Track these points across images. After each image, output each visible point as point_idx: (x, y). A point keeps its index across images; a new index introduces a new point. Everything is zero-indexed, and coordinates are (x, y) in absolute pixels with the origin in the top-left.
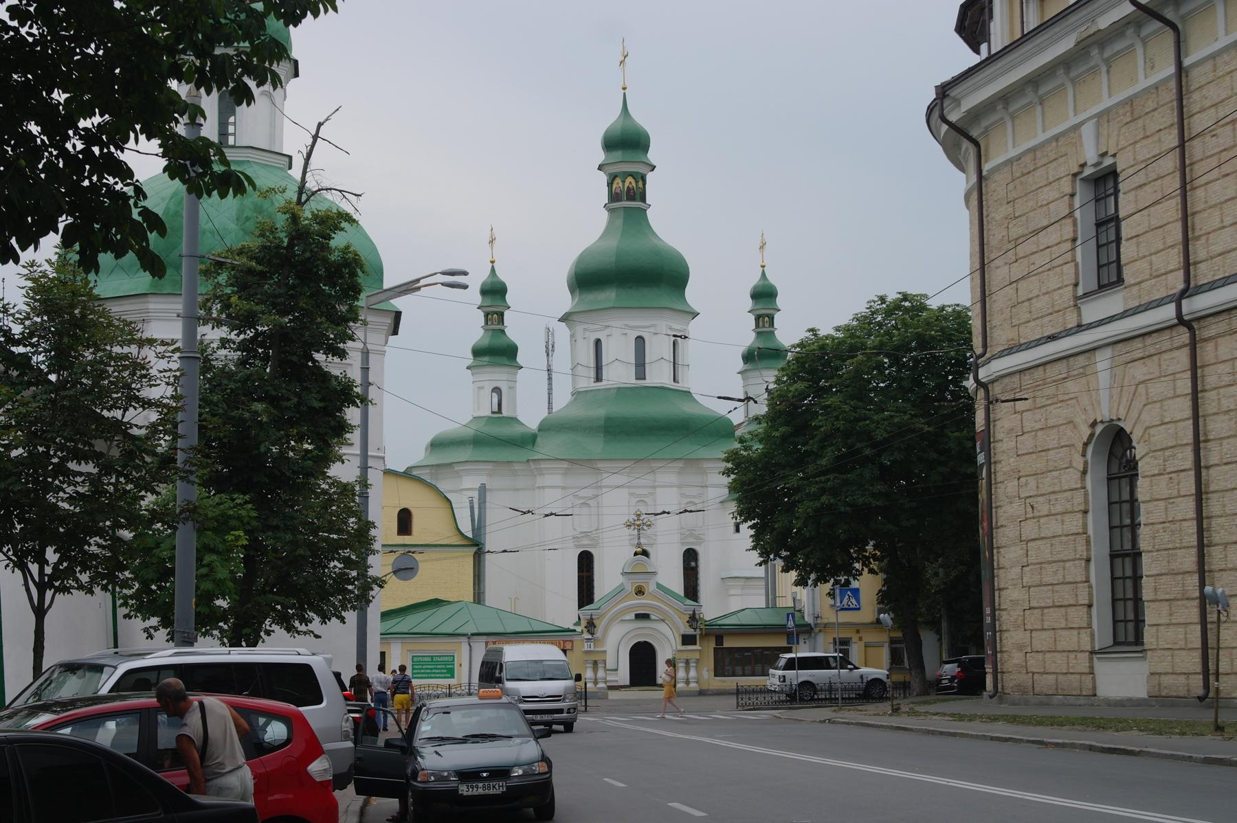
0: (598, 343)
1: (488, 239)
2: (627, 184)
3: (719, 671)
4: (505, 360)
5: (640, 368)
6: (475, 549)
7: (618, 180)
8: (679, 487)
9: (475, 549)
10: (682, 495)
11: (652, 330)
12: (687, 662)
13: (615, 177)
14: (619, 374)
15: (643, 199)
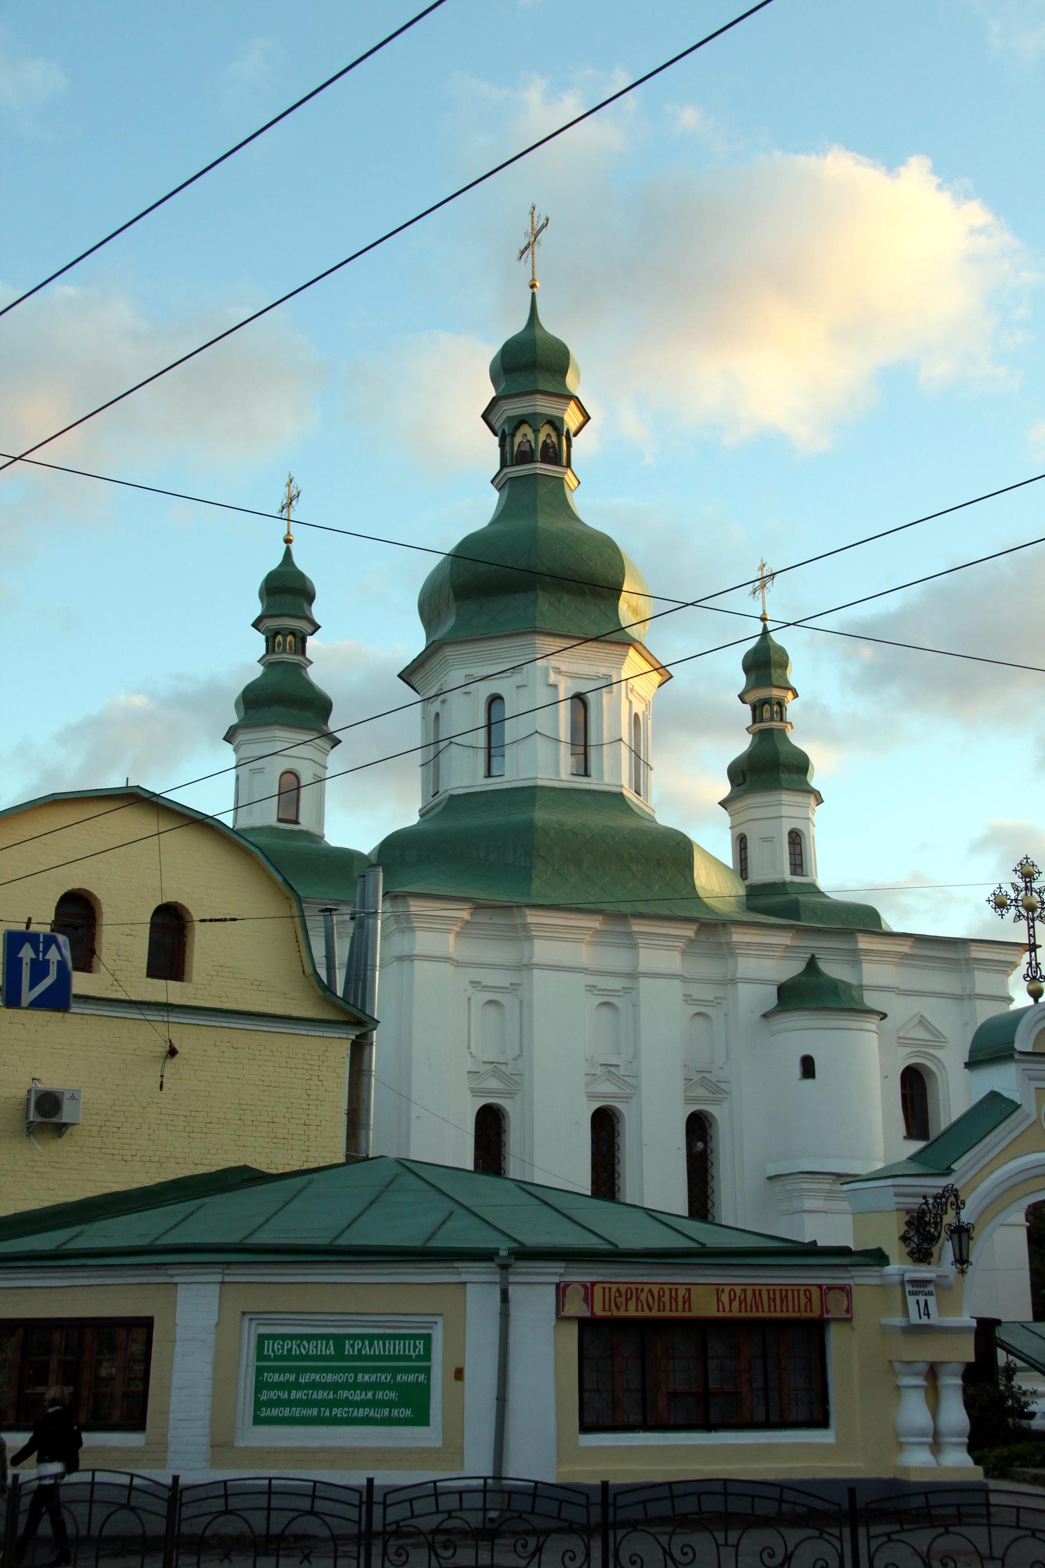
2: (542, 437)
7: (525, 429)
8: (684, 979)
10: (688, 998)
13: (517, 428)
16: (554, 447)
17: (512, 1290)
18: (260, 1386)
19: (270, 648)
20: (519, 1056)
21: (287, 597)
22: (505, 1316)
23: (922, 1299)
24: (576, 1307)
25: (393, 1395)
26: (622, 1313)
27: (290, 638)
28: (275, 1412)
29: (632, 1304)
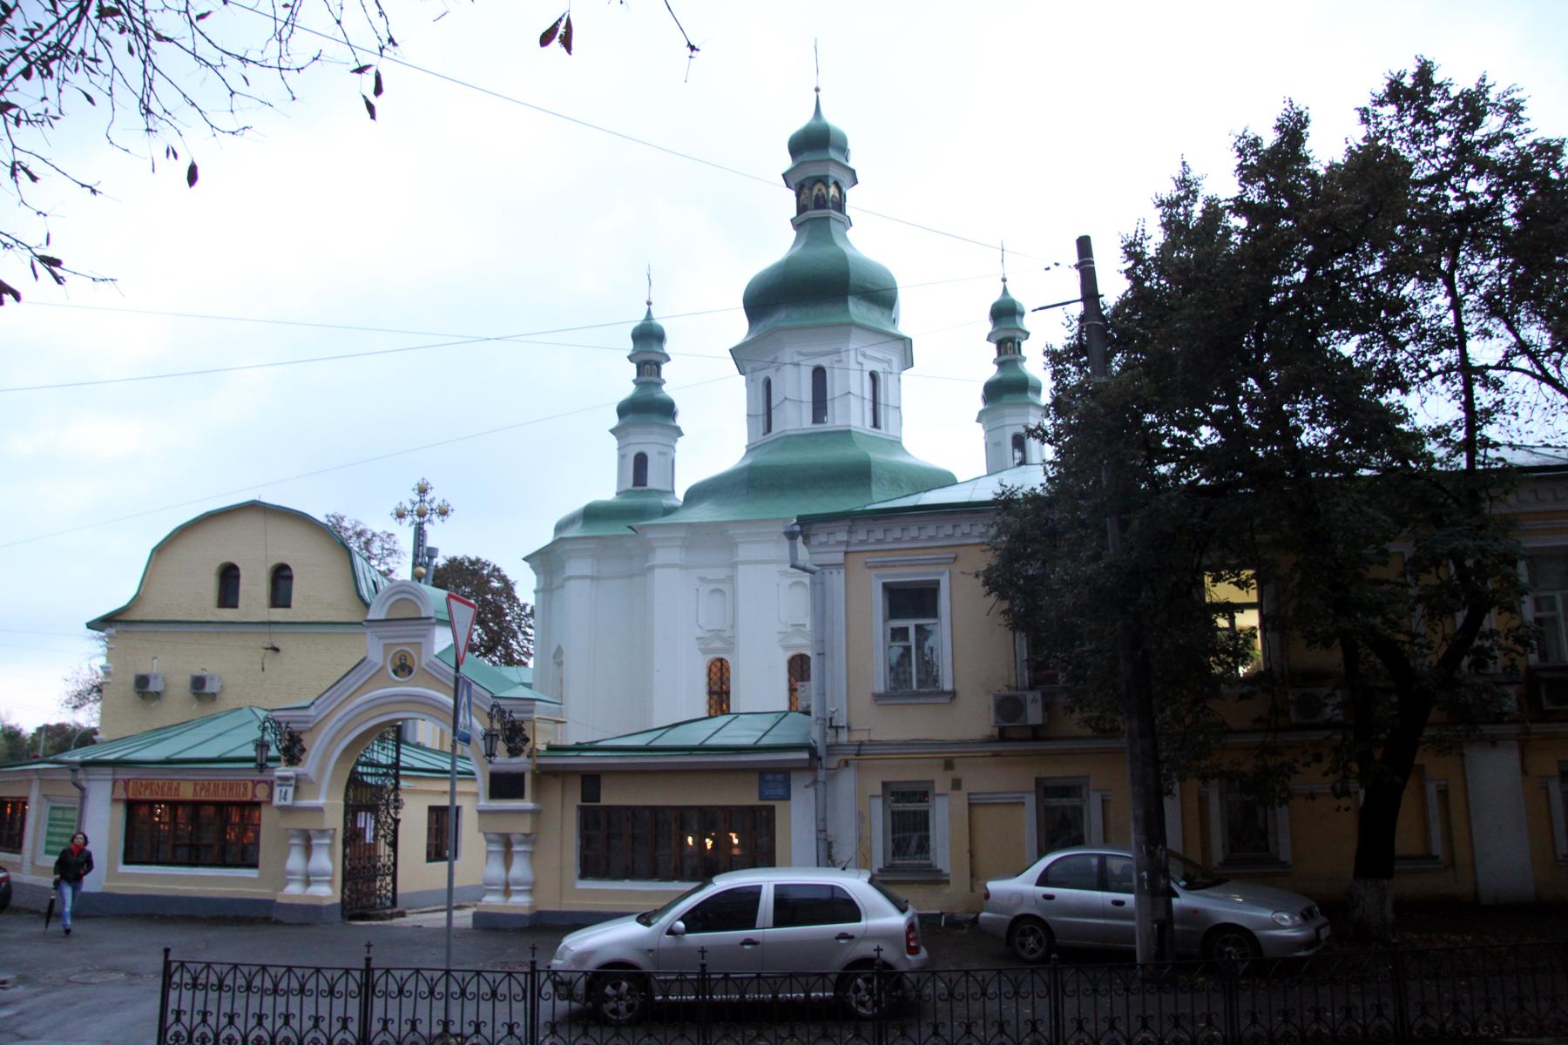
4: (656, 418)
5: (820, 407)
11: (835, 357)
12: (507, 842)
14: (795, 417)
17: (84, 784)
20: (733, 626)
21: (648, 339)
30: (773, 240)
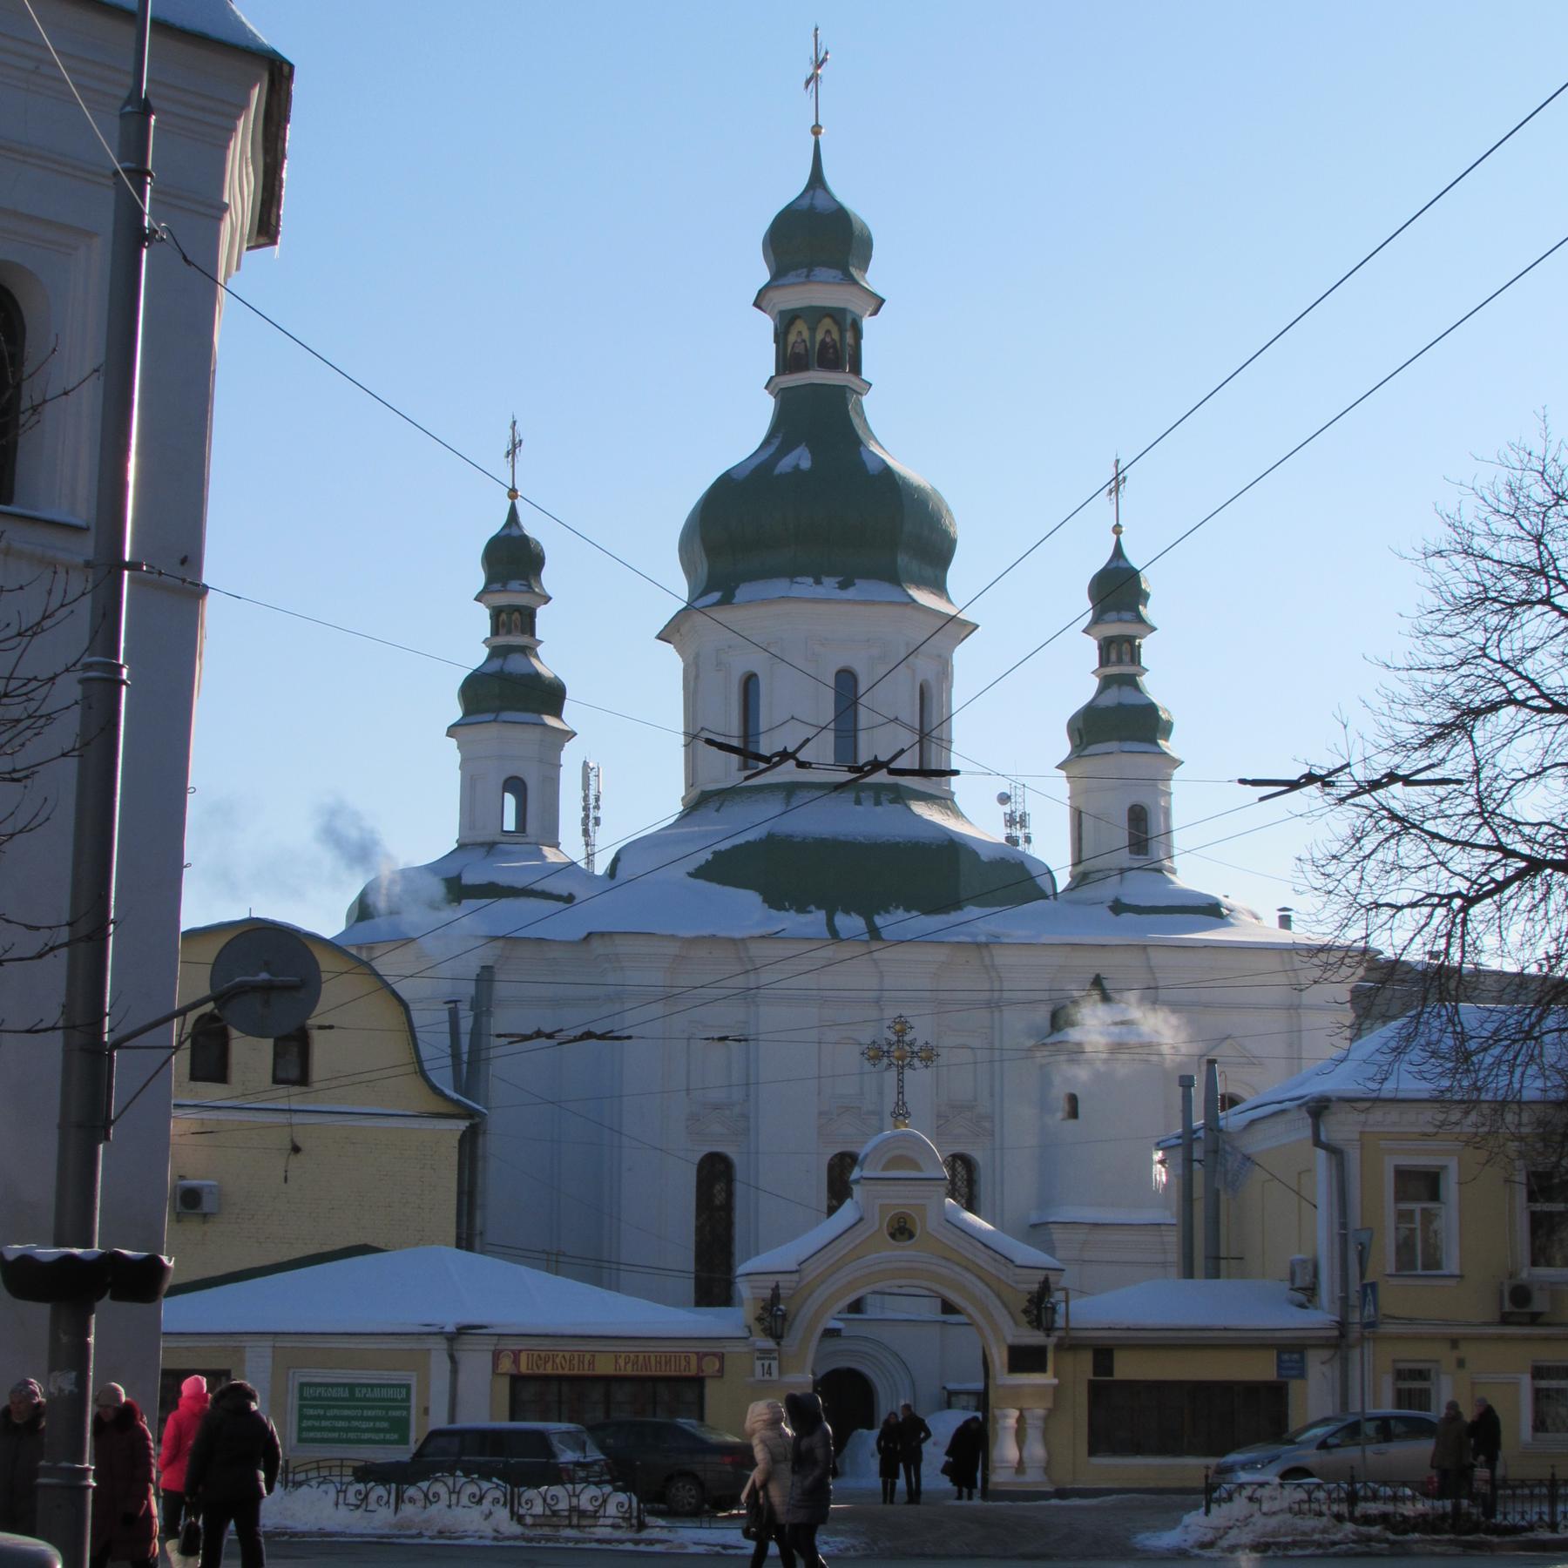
0: (750, 684)
1: (506, 445)
2: (819, 336)
3: (1100, 1442)
6: (463, 1125)
7: (801, 326)
9: (463, 1125)
15: (856, 369)
16: (834, 346)
17: (458, 1355)
18: (302, 1417)
19: (495, 631)
21: (513, 561)
22: (454, 1371)
23: (766, 1363)
24: (506, 1365)
25: (385, 1425)
26: (542, 1371)
27: (516, 616)
28: (312, 1435)
29: (549, 1366)
30: (735, 420)
